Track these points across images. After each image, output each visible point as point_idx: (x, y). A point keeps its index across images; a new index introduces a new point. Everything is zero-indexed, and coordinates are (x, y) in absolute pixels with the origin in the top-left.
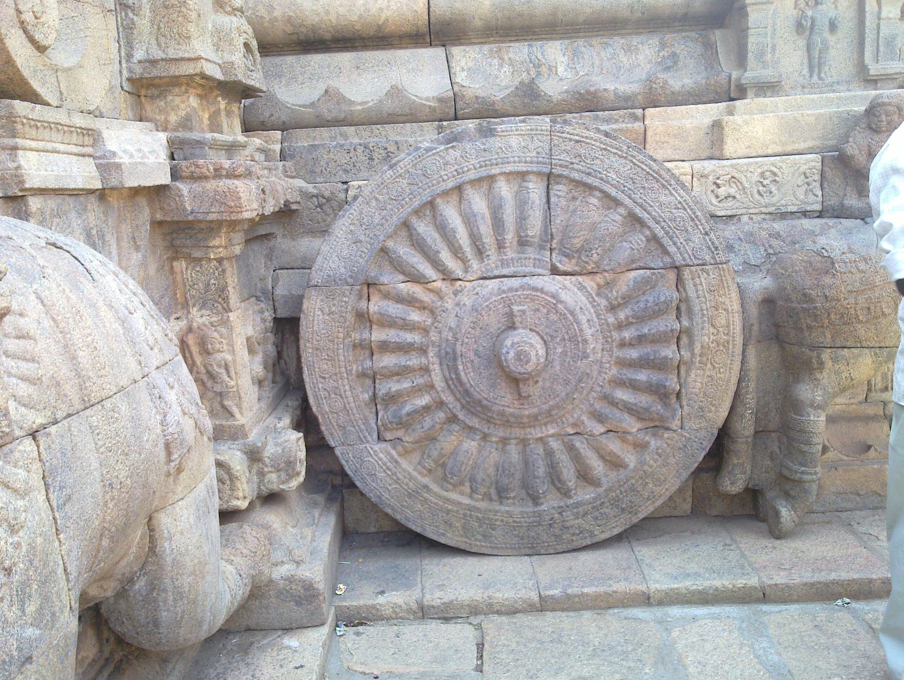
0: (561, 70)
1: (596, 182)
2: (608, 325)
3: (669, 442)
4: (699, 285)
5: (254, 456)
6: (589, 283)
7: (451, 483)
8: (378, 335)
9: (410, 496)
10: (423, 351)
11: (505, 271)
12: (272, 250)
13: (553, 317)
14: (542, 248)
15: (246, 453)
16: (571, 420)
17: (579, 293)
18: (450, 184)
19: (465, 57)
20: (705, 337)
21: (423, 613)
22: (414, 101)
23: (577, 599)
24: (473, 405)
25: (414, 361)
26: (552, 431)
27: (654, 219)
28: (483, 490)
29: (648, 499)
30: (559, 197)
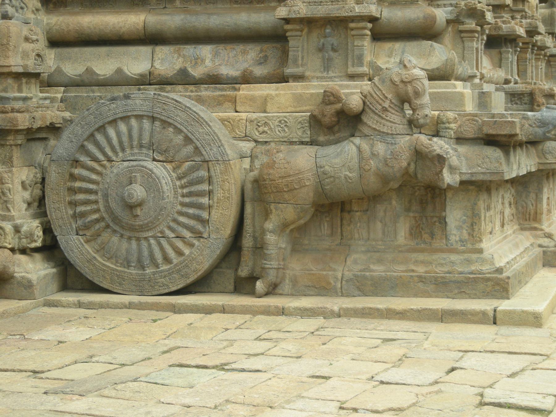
0: (207, 61)
1: (172, 121)
2: (176, 186)
3: (203, 244)
4: (216, 170)
5: (17, 229)
6: (169, 166)
7: (106, 257)
8: (78, 184)
9: (88, 261)
10: (96, 192)
11: (132, 158)
12: (47, 145)
13: (150, 180)
14: (149, 149)
15: (13, 227)
16: (159, 230)
17: (164, 170)
18: (111, 119)
19: (162, 51)
20: (219, 194)
21: (80, 305)
22: (128, 75)
23: (144, 305)
24: (116, 219)
25: (93, 197)
26: (150, 235)
27: (196, 139)
28: (120, 261)
29: (194, 271)
30: (156, 127)
